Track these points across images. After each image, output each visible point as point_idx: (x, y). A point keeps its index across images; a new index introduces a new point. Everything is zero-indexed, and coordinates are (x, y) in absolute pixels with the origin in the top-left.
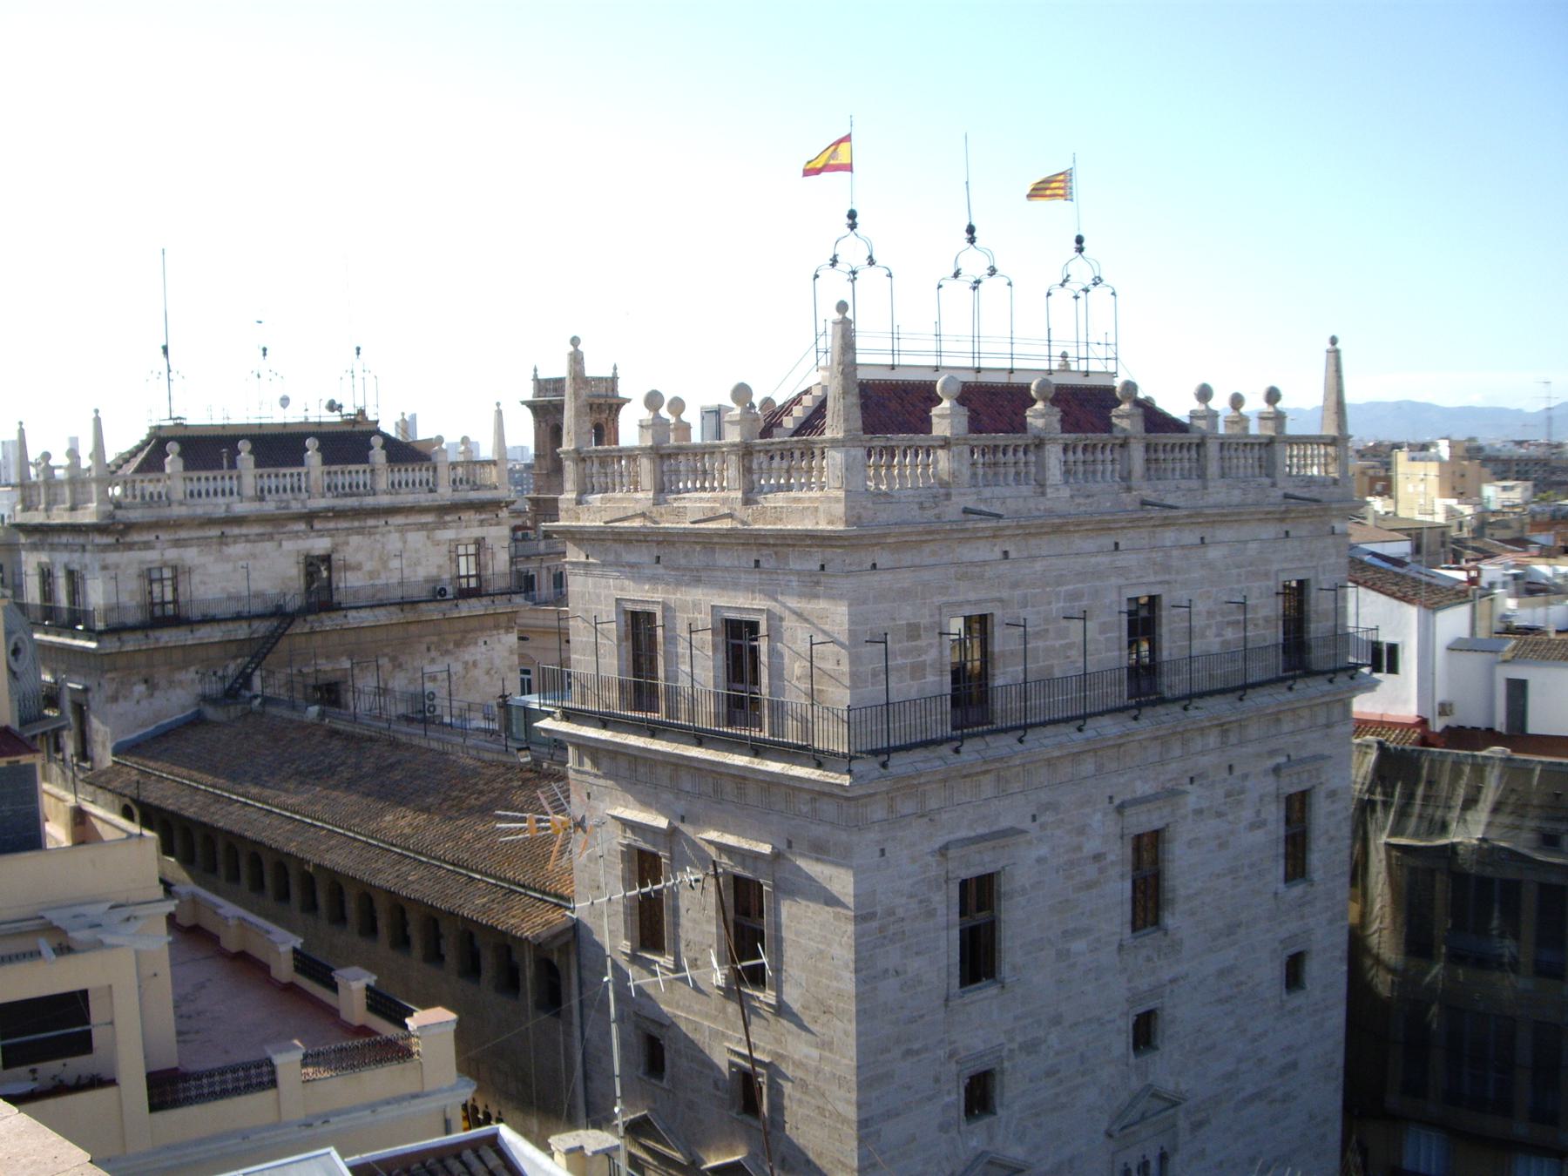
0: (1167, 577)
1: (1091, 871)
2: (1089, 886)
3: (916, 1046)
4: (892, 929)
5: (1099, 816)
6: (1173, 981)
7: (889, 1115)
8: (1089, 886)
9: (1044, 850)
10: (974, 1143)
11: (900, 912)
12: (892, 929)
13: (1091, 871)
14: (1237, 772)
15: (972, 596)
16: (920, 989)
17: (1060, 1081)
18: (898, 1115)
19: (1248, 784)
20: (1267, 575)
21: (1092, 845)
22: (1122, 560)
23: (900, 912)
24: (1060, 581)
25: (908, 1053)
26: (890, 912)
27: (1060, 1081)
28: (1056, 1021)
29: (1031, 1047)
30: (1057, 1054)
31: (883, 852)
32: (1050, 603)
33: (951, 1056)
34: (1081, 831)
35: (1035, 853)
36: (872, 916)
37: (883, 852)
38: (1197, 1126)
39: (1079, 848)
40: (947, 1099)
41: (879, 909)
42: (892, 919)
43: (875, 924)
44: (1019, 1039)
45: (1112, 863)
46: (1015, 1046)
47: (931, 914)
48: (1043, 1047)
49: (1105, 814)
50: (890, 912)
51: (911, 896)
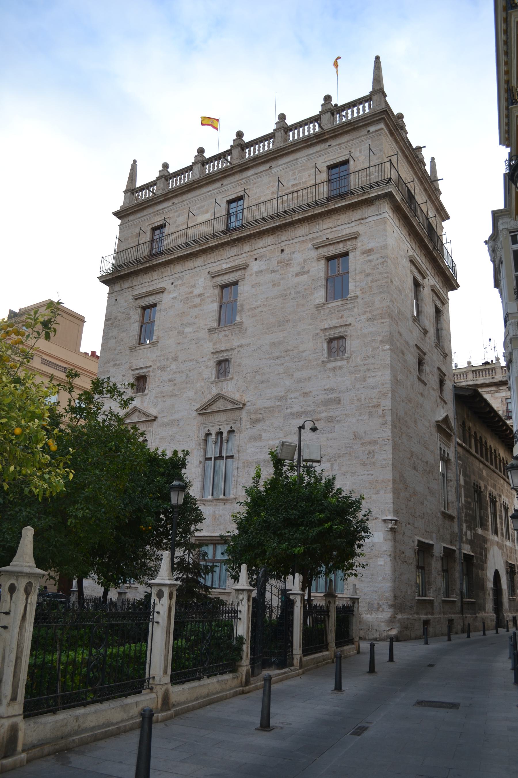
1: (197, 300)
2: (195, 306)
3: (118, 362)
5: (202, 280)
6: (241, 346)
9: (175, 295)
11: (119, 318)
13: (197, 300)
16: (122, 343)
17: (175, 384)
19: (295, 256)
21: (197, 291)
23: (119, 318)
26: (116, 318)
28: (175, 359)
30: (175, 373)
31: (116, 300)
34: (194, 286)
35: (171, 296)
37: (116, 300)
38: (255, 422)
39: (192, 292)
41: (112, 317)
43: (110, 322)
44: (158, 364)
45: (208, 297)
46: (156, 367)
48: (168, 369)
49: (205, 279)
50: (116, 318)
51: (123, 313)
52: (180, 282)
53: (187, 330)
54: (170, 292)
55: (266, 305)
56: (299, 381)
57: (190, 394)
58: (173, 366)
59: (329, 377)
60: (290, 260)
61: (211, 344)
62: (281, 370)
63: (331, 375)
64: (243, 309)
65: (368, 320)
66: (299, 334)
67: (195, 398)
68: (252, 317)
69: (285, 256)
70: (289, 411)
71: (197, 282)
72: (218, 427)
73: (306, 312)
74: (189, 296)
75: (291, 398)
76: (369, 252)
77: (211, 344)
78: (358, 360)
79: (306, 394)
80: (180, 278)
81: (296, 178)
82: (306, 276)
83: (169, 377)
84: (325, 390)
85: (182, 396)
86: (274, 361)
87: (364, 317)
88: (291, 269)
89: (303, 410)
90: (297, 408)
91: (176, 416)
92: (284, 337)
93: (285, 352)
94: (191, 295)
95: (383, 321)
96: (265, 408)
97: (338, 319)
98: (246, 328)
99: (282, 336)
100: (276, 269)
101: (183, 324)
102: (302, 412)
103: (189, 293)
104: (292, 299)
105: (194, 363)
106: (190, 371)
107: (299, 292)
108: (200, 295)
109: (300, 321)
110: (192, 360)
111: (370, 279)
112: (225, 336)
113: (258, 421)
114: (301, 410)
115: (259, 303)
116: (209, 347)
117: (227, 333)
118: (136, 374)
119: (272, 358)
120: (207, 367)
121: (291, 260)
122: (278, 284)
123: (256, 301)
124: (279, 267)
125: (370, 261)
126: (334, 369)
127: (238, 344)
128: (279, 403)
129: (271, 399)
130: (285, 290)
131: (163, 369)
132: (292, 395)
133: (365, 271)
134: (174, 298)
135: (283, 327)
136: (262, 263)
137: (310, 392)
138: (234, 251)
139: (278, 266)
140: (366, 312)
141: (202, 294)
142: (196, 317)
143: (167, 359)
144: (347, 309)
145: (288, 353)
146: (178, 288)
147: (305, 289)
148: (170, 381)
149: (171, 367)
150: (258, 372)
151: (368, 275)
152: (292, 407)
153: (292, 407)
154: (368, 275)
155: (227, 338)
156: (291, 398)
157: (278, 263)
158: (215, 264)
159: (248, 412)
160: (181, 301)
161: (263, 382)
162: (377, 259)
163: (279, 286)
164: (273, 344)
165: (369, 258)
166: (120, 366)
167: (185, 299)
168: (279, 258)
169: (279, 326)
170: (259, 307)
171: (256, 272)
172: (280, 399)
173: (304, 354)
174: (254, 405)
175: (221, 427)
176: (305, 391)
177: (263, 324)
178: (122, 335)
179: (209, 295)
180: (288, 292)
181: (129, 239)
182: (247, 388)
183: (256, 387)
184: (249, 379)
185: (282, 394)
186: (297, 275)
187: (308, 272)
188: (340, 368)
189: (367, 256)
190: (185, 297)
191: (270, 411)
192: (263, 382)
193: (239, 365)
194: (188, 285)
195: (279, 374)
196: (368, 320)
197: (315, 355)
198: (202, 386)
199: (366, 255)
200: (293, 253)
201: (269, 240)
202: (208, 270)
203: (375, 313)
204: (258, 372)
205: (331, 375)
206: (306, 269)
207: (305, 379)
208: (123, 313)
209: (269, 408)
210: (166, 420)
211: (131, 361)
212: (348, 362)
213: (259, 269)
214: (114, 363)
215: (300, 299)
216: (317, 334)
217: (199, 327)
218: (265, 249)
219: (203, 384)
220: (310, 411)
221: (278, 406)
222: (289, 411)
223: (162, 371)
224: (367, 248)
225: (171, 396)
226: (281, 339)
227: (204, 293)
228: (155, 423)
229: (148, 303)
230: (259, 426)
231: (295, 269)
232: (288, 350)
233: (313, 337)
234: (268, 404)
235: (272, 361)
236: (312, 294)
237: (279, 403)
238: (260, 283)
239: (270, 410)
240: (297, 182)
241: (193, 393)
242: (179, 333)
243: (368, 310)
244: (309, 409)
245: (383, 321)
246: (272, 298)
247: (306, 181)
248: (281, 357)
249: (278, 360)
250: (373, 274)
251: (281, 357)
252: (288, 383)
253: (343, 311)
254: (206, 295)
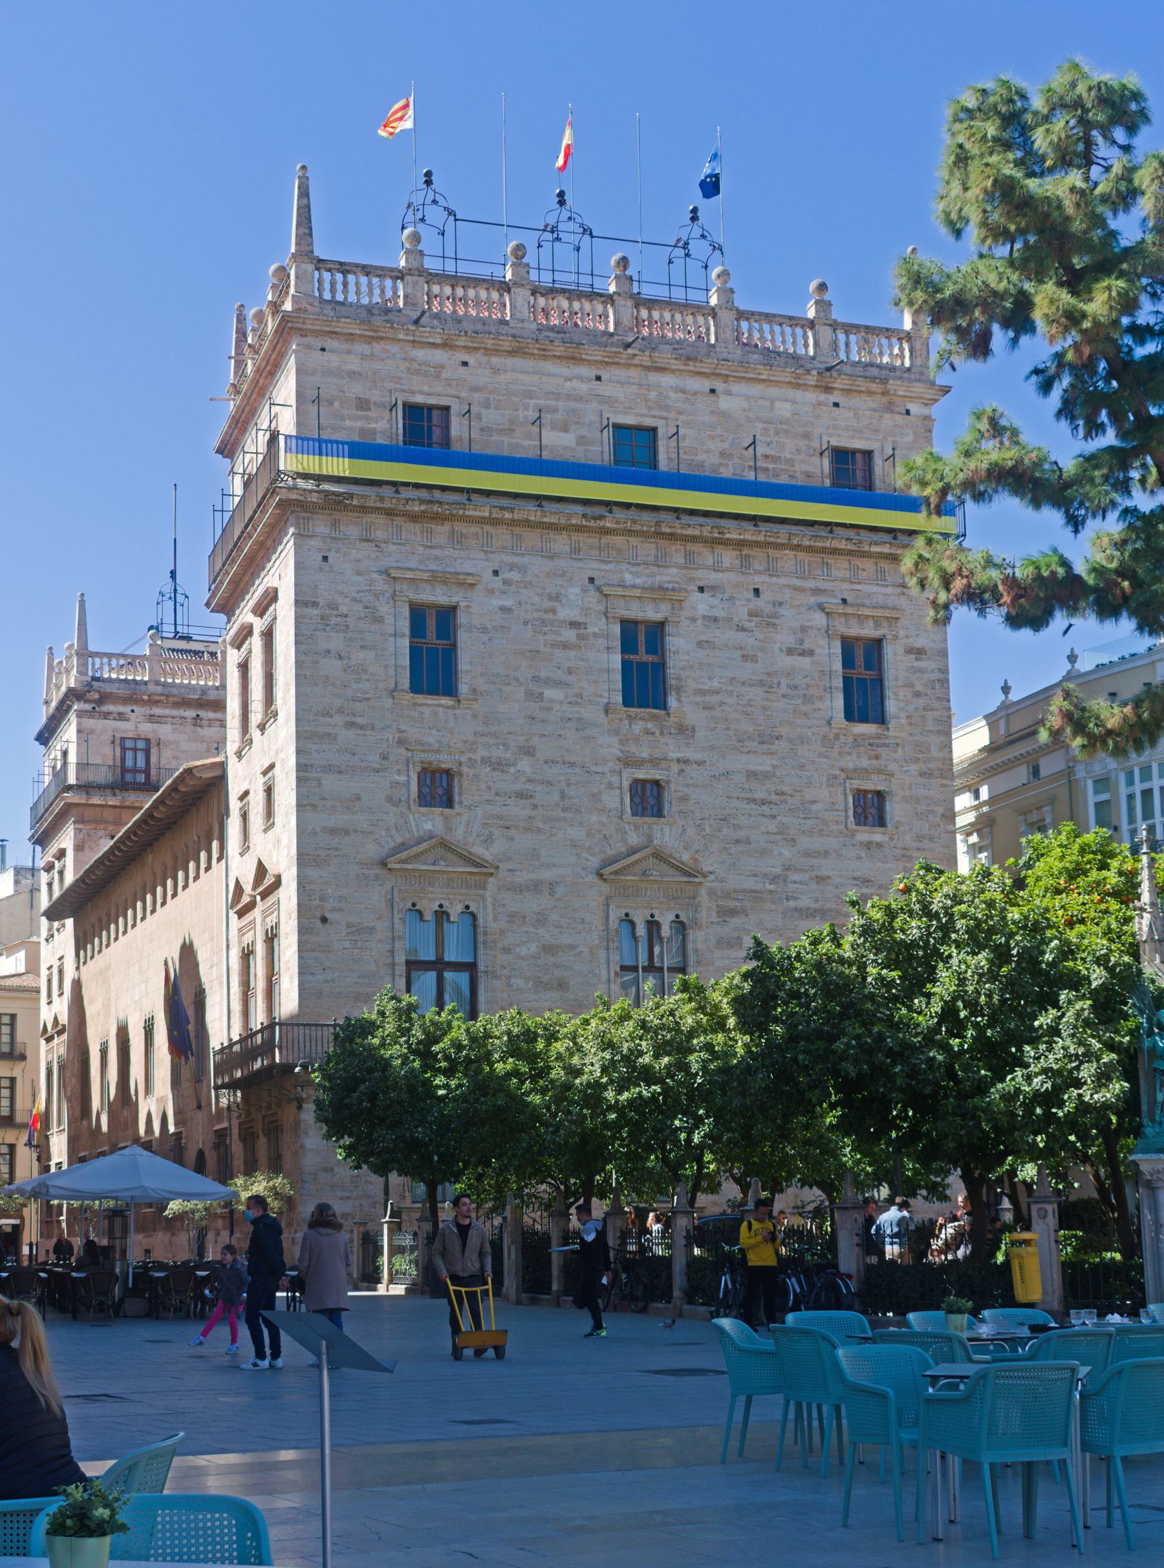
0: (665, 414)
2: (565, 646)
3: (360, 721)
4: (333, 620)
5: (577, 590)
7: (328, 769)
8: (565, 646)
9: (508, 603)
10: (428, 826)
11: (343, 609)
12: (333, 620)
13: (570, 635)
14: (766, 596)
15: (426, 389)
16: (364, 677)
17: (535, 807)
18: (340, 773)
19: (782, 611)
20: (807, 436)
21: (564, 614)
22: (603, 389)
24: (529, 394)
25: (351, 725)
27: (535, 807)
28: (529, 752)
29: (499, 766)
30: (529, 780)
31: (325, 558)
32: (517, 410)
33: (400, 742)
36: (315, 604)
37: (325, 558)
38: (726, 913)
39: (553, 611)
40: (396, 777)
41: (321, 602)
42: (335, 612)
43: (316, 612)
44: (481, 753)
45: (595, 635)
46: (477, 757)
47: (378, 620)
48: (512, 769)
50: (333, 606)
51: (354, 600)
52: (515, 576)
53: (549, 693)
54: (491, 592)
55: (732, 692)
56: (808, 854)
57: (577, 833)
58: (525, 765)
59: (860, 858)
60: (775, 616)
61: (615, 740)
62: (772, 828)
63: (863, 855)
64: (682, 687)
65: (922, 774)
66: (802, 767)
67: (587, 845)
68: (704, 708)
69: (760, 603)
70: (791, 903)
71: (563, 592)
72: (648, 913)
73: (813, 730)
74: (544, 616)
75: (795, 882)
76: (920, 652)
77: (615, 740)
78: (908, 838)
79: (821, 879)
80: (512, 567)
81: (771, 442)
82: (807, 660)
83: (518, 787)
84: (855, 879)
85: (554, 835)
86: (757, 807)
87: (914, 768)
88: (779, 637)
89: (817, 906)
90: (805, 902)
91: (546, 875)
92: (774, 767)
93: (777, 794)
94: (550, 616)
95: (944, 782)
96: (744, 891)
97: (870, 758)
98: (693, 728)
99: (768, 762)
100: (747, 625)
101: (538, 677)
102: (816, 911)
103: (546, 611)
104: (783, 696)
105: (578, 770)
106: (569, 785)
107: (796, 687)
108: (574, 624)
109: (802, 743)
110: (572, 765)
111: (921, 702)
112: (648, 732)
113: (733, 912)
114: (814, 906)
115: (716, 684)
116: (610, 747)
117: (650, 725)
118: (422, 762)
119: (754, 801)
120: (610, 786)
121: (776, 617)
122: (754, 659)
123: (710, 678)
124: (753, 624)
125: (920, 670)
126: (868, 845)
127: (679, 755)
128: (772, 887)
129: (755, 875)
130: (769, 674)
131: (499, 766)
132: (796, 877)
133: (912, 686)
134: (503, 609)
135: (771, 747)
136: (715, 601)
137: (829, 877)
138: (647, 550)
139: (750, 621)
140: (917, 760)
141: (579, 624)
142: (570, 671)
143: (506, 746)
144: (887, 745)
145: (783, 798)
146: (513, 588)
147: (808, 686)
148: (520, 795)
149: (519, 767)
150: (725, 820)
151: (917, 695)
152: (796, 898)
153: (796, 898)
154: (917, 695)
155: (650, 738)
156: (795, 882)
157: (751, 614)
158: (604, 567)
159: (712, 893)
160: (526, 623)
161: (738, 841)
162: (933, 671)
163: (756, 662)
164: (752, 775)
165: (917, 664)
166: (368, 732)
167: (535, 620)
168: (752, 606)
169: (762, 743)
170: (717, 693)
171: (704, 617)
172: (774, 879)
173: (814, 807)
174: (722, 881)
175: (656, 913)
176: (819, 874)
177: (728, 729)
178: (361, 655)
179: (596, 630)
180: (775, 681)
181: (336, 404)
182: (706, 847)
183: (724, 848)
184: (708, 830)
185: (778, 871)
186: (790, 652)
187: (811, 653)
188: (879, 845)
189: (917, 659)
190: (535, 615)
191: (756, 898)
192: (738, 841)
193: (685, 799)
194: (539, 591)
195: (768, 833)
196: (922, 774)
197: (835, 813)
198: (604, 824)
199: (913, 656)
200: (780, 604)
201: (728, 557)
202: (590, 574)
203: (931, 765)
204: (725, 820)
205: (863, 855)
206: (807, 645)
207: (819, 853)
208: (354, 600)
209: (752, 891)
210: (520, 878)
211: (403, 728)
212: (891, 839)
213: (710, 614)
214: (347, 719)
215: (800, 702)
216: (836, 777)
217: (580, 696)
218: (719, 575)
219: (604, 820)
220: (830, 910)
221: (771, 892)
222: (791, 903)
223: (494, 769)
224: (916, 645)
225: (527, 830)
226: (769, 769)
227: (586, 624)
228: (491, 879)
229: (434, 598)
230: (735, 921)
231: (785, 639)
232: (783, 793)
233: (828, 780)
234: (750, 884)
235: (752, 806)
236: (821, 698)
237: (772, 887)
238: (713, 643)
239: (756, 896)
240: (773, 453)
241: (583, 833)
242: (529, 694)
243: (921, 756)
244: (828, 905)
245: (944, 782)
246: (744, 683)
247: (792, 460)
248: (770, 803)
249: (764, 808)
250: (926, 695)
251: (770, 803)
252: (787, 853)
253: (879, 746)
254: (592, 629)
